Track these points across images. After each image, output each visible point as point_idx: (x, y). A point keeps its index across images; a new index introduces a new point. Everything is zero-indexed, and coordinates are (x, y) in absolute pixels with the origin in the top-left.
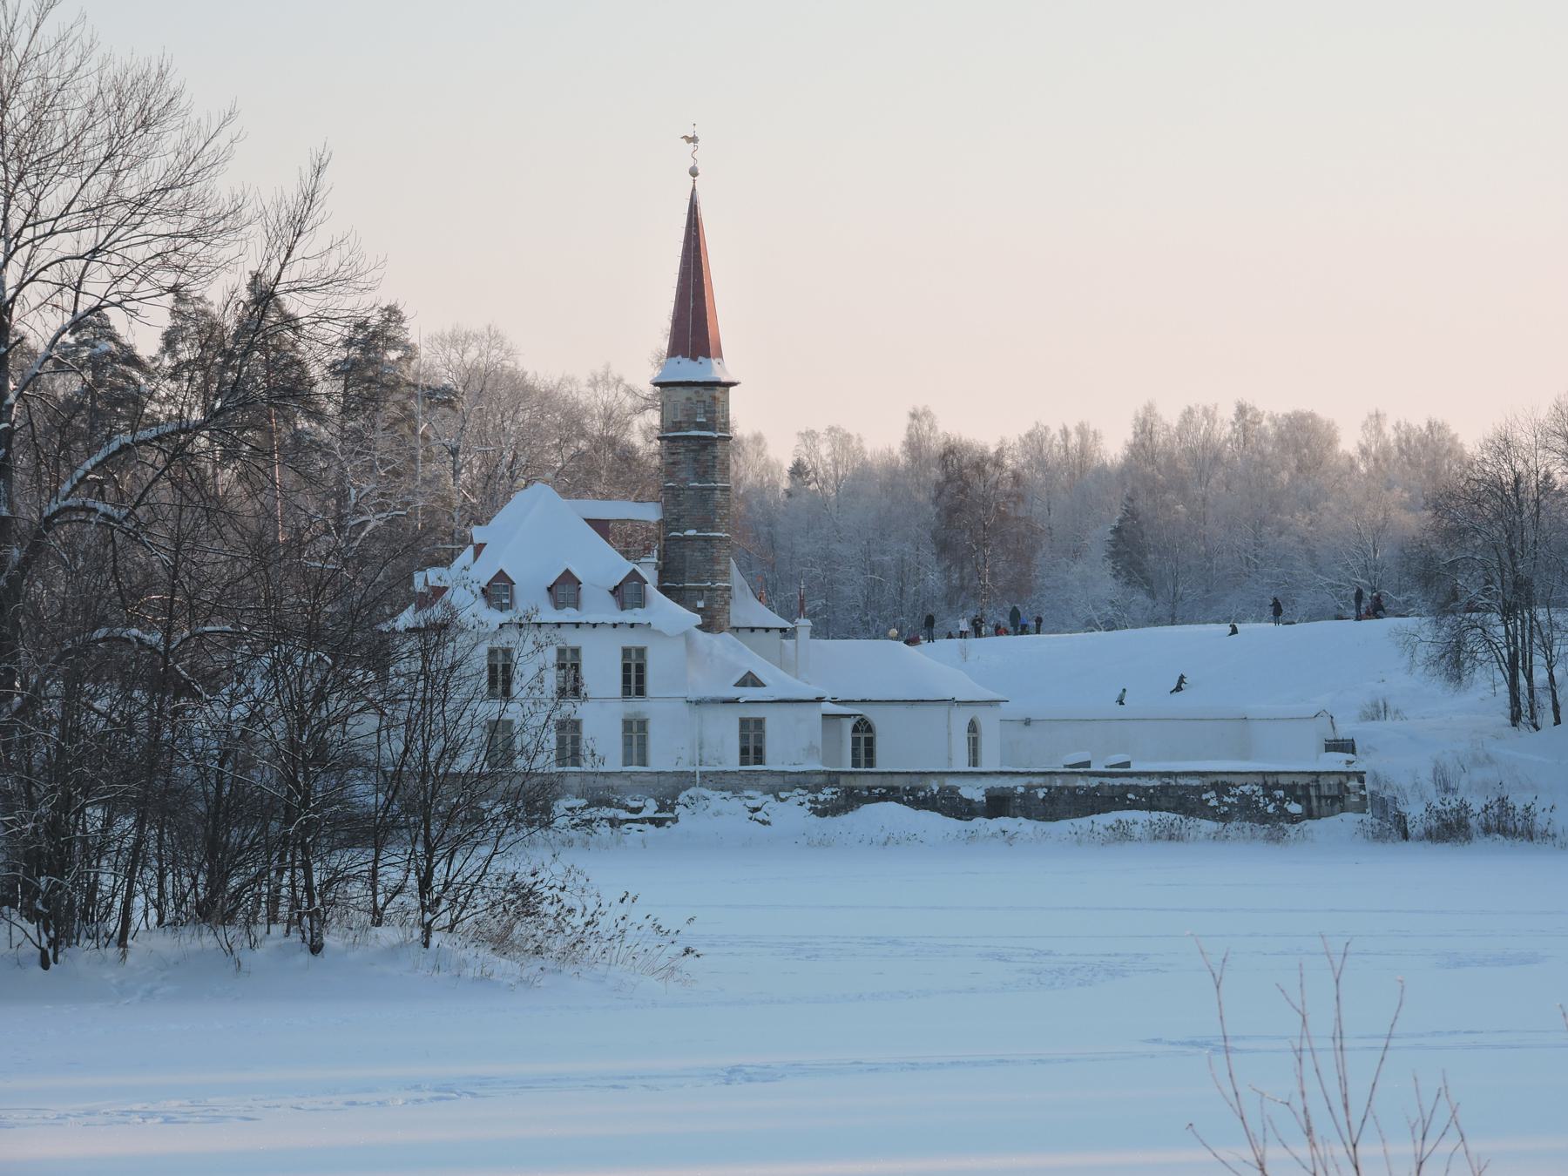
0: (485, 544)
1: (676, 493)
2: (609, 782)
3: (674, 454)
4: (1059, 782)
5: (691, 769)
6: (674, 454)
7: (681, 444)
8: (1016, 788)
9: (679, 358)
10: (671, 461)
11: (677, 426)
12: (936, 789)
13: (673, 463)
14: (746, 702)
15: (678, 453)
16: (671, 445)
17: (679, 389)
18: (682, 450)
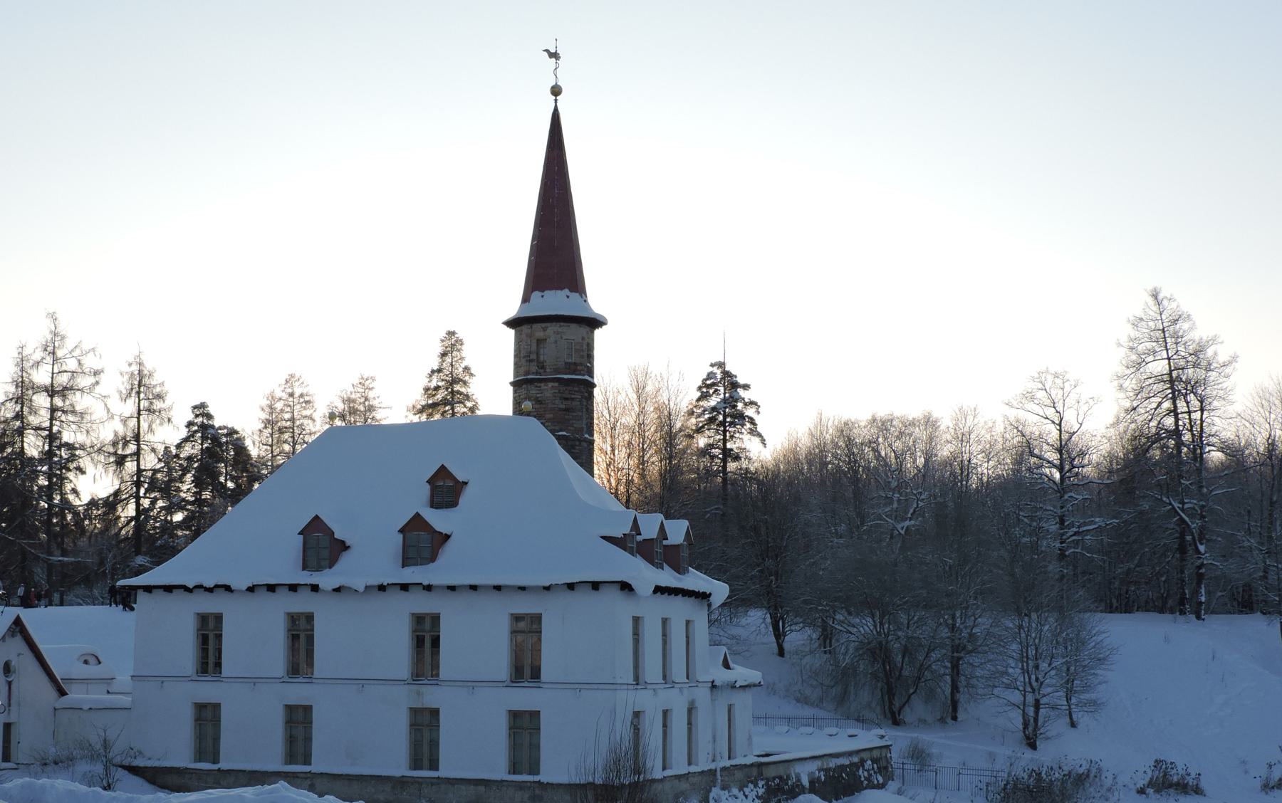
0: (466, 483)
1: (570, 443)
2: (684, 786)
3: (566, 399)
4: (833, 763)
5: (712, 766)
6: (566, 399)
7: (576, 389)
8: (814, 773)
9: (567, 291)
10: (563, 406)
11: (572, 368)
12: (794, 777)
13: (567, 410)
14: (741, 687)
15: (573, 399)
16: (562, 389)
17: (573, 326)
18: (578, 396)
